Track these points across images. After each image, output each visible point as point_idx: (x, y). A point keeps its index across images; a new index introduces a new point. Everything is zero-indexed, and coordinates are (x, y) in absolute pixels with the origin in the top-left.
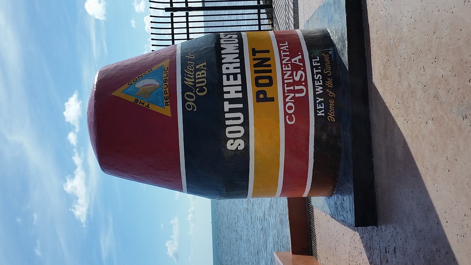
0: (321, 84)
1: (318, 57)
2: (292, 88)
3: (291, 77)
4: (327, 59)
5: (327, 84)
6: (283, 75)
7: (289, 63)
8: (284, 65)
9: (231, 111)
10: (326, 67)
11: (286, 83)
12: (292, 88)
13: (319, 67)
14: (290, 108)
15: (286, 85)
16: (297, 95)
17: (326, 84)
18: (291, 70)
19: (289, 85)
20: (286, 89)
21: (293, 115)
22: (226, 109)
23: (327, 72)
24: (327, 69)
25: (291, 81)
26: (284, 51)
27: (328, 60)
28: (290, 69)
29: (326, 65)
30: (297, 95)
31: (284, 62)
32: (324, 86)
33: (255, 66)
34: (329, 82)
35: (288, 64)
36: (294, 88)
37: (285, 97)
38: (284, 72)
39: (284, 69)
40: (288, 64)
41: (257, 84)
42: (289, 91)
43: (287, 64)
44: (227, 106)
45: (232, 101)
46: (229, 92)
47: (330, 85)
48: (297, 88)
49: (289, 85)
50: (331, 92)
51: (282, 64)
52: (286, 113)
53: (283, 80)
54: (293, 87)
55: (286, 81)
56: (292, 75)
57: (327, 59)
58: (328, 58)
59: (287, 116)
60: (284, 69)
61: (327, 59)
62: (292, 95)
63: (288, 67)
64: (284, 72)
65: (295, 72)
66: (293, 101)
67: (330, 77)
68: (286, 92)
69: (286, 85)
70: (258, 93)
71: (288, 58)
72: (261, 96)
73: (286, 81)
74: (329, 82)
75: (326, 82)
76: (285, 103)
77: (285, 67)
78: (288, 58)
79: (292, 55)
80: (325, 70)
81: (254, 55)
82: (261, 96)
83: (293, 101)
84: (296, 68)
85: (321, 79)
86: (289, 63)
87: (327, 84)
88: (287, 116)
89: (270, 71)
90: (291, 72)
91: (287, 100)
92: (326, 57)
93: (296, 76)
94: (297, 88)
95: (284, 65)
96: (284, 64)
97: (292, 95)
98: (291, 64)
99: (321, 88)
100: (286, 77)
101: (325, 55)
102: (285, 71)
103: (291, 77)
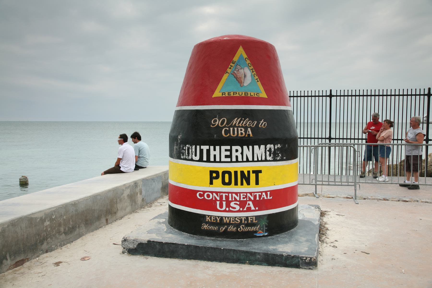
0: (231, 222)
1: (256, 222)
2: (224, 199)
3: (233, 200)
4: (253, 229)
5: (231, 227)
6: (236, 194)
7: (247, 199)
8: (245, 194)
9: (201, 151)
10: (247, 228)
11: (229, 195)
12: (224, 199)
13: (246, 222)
14: (208, 196)
15: (227, 194)
16: (218, 203)
17: (231, 226)
18: (241, 200)
19: (227, 197)
20: (224, 195)
21: (203, 198)
22: (202, 147)
23: (242, 229)
24: (244, 228)
25: (230, 199)
26: (260, 196)
27: (253, 230)
28: (242, 199)
29: (249, 228)
30: (218, 203)
31: (249, 195)
32: (229, 224)
33: (242, 172)
34: (232, 228)
35: (246, 198)
36: (224, 201)
37: (217, 193)
38: (239, 194)
39: (242, 194)
40: (246, 198)
41: (224, 173)
42: (221, 197)
43: (246, 196)
44: (205, 148)
45: (208, 151)
46: (215, 150)
47: (230, 228)
48: (224, 203)
49: (227, 197)
50: (224, 229)
51: (246, 193)
52: (204, 192)
53: (232, 193)
54: (225, 200)
55: (230, 195)
56: (236, 200)
57: (253, 229)
58: (255, 230)
59: (202, 193)
60: (242, 194)
61: (254, 229)
62: (218, 199)
63: (244, 198)
64: (239, 194)
65: (238, 203)
66: (214, 199)
67: (237, 229)
68: (221, 194)
69: (227, 194)
70: (217, 172)
71: (252, 198)
72: (214, 175)
73: (230, 195)
74: (232, 228)
75: (233, 226)
76: (212, 192)
77: (243, 195)
78: (252, 198)
79: (255, 202)
80: (244, 226)
81: (254, 172)
82: (214, 175)
83: (214, 199)
84: (242, 204)
85: (236, 222)
86: (247, 199)
87: (231, 227)
88: (202, 193)
89: (236, 184)
90: (238, 198)
91: (214, 194)
92: (256, 229)
93: (235, 204)
94: (224, 203)
95: (245, 194)
96: (247, 195)
97: (218, 199)
98: (247, 201)
99: (228, 222)
100: (234, 195)
101: (258, 227)
102: (240, 195)
103: (233, 200)
